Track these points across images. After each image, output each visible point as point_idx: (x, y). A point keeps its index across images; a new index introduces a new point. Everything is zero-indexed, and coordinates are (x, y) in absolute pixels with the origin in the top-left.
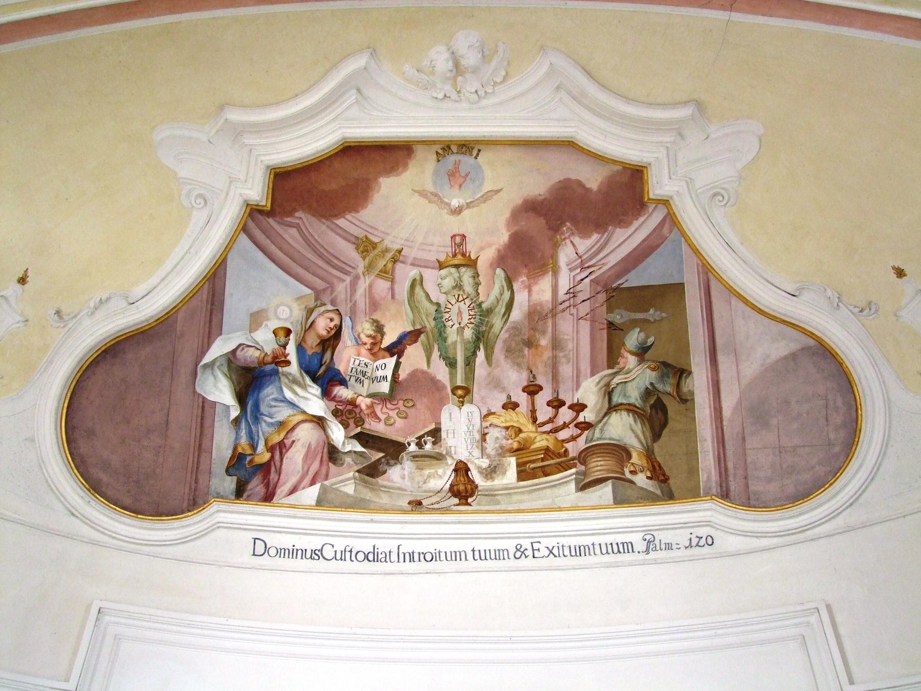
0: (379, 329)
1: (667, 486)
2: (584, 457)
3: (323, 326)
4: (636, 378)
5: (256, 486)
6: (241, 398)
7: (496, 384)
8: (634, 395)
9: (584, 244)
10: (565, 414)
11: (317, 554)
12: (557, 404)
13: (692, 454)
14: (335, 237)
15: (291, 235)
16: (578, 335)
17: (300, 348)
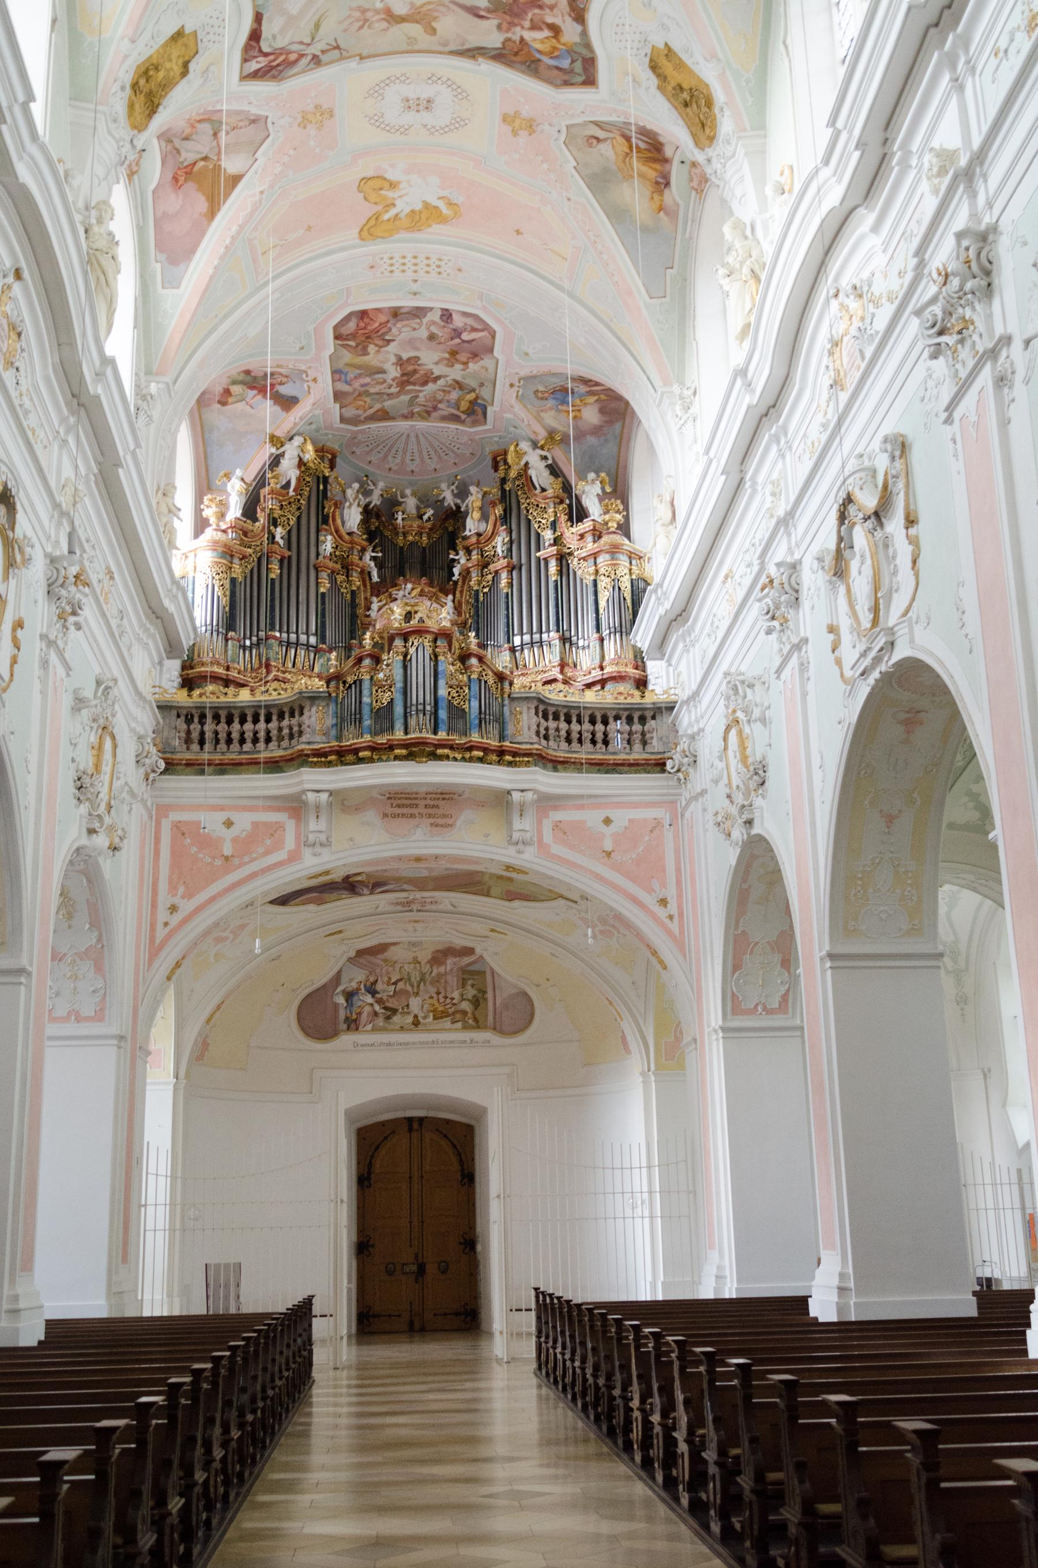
0: (390, 979)
1: (478, 1024)
2: (454, 1013)
3: (372, 979)
4: (471, 992)
5: (353, 1025)
6: (347, 1001)
8: (470, 997)
9: (455, 960)
10: (448, 1001)
11: (373, 1045)
13: (487, 1016)
14: (378, 960)
15: (361, 960)
16: (453, 981)
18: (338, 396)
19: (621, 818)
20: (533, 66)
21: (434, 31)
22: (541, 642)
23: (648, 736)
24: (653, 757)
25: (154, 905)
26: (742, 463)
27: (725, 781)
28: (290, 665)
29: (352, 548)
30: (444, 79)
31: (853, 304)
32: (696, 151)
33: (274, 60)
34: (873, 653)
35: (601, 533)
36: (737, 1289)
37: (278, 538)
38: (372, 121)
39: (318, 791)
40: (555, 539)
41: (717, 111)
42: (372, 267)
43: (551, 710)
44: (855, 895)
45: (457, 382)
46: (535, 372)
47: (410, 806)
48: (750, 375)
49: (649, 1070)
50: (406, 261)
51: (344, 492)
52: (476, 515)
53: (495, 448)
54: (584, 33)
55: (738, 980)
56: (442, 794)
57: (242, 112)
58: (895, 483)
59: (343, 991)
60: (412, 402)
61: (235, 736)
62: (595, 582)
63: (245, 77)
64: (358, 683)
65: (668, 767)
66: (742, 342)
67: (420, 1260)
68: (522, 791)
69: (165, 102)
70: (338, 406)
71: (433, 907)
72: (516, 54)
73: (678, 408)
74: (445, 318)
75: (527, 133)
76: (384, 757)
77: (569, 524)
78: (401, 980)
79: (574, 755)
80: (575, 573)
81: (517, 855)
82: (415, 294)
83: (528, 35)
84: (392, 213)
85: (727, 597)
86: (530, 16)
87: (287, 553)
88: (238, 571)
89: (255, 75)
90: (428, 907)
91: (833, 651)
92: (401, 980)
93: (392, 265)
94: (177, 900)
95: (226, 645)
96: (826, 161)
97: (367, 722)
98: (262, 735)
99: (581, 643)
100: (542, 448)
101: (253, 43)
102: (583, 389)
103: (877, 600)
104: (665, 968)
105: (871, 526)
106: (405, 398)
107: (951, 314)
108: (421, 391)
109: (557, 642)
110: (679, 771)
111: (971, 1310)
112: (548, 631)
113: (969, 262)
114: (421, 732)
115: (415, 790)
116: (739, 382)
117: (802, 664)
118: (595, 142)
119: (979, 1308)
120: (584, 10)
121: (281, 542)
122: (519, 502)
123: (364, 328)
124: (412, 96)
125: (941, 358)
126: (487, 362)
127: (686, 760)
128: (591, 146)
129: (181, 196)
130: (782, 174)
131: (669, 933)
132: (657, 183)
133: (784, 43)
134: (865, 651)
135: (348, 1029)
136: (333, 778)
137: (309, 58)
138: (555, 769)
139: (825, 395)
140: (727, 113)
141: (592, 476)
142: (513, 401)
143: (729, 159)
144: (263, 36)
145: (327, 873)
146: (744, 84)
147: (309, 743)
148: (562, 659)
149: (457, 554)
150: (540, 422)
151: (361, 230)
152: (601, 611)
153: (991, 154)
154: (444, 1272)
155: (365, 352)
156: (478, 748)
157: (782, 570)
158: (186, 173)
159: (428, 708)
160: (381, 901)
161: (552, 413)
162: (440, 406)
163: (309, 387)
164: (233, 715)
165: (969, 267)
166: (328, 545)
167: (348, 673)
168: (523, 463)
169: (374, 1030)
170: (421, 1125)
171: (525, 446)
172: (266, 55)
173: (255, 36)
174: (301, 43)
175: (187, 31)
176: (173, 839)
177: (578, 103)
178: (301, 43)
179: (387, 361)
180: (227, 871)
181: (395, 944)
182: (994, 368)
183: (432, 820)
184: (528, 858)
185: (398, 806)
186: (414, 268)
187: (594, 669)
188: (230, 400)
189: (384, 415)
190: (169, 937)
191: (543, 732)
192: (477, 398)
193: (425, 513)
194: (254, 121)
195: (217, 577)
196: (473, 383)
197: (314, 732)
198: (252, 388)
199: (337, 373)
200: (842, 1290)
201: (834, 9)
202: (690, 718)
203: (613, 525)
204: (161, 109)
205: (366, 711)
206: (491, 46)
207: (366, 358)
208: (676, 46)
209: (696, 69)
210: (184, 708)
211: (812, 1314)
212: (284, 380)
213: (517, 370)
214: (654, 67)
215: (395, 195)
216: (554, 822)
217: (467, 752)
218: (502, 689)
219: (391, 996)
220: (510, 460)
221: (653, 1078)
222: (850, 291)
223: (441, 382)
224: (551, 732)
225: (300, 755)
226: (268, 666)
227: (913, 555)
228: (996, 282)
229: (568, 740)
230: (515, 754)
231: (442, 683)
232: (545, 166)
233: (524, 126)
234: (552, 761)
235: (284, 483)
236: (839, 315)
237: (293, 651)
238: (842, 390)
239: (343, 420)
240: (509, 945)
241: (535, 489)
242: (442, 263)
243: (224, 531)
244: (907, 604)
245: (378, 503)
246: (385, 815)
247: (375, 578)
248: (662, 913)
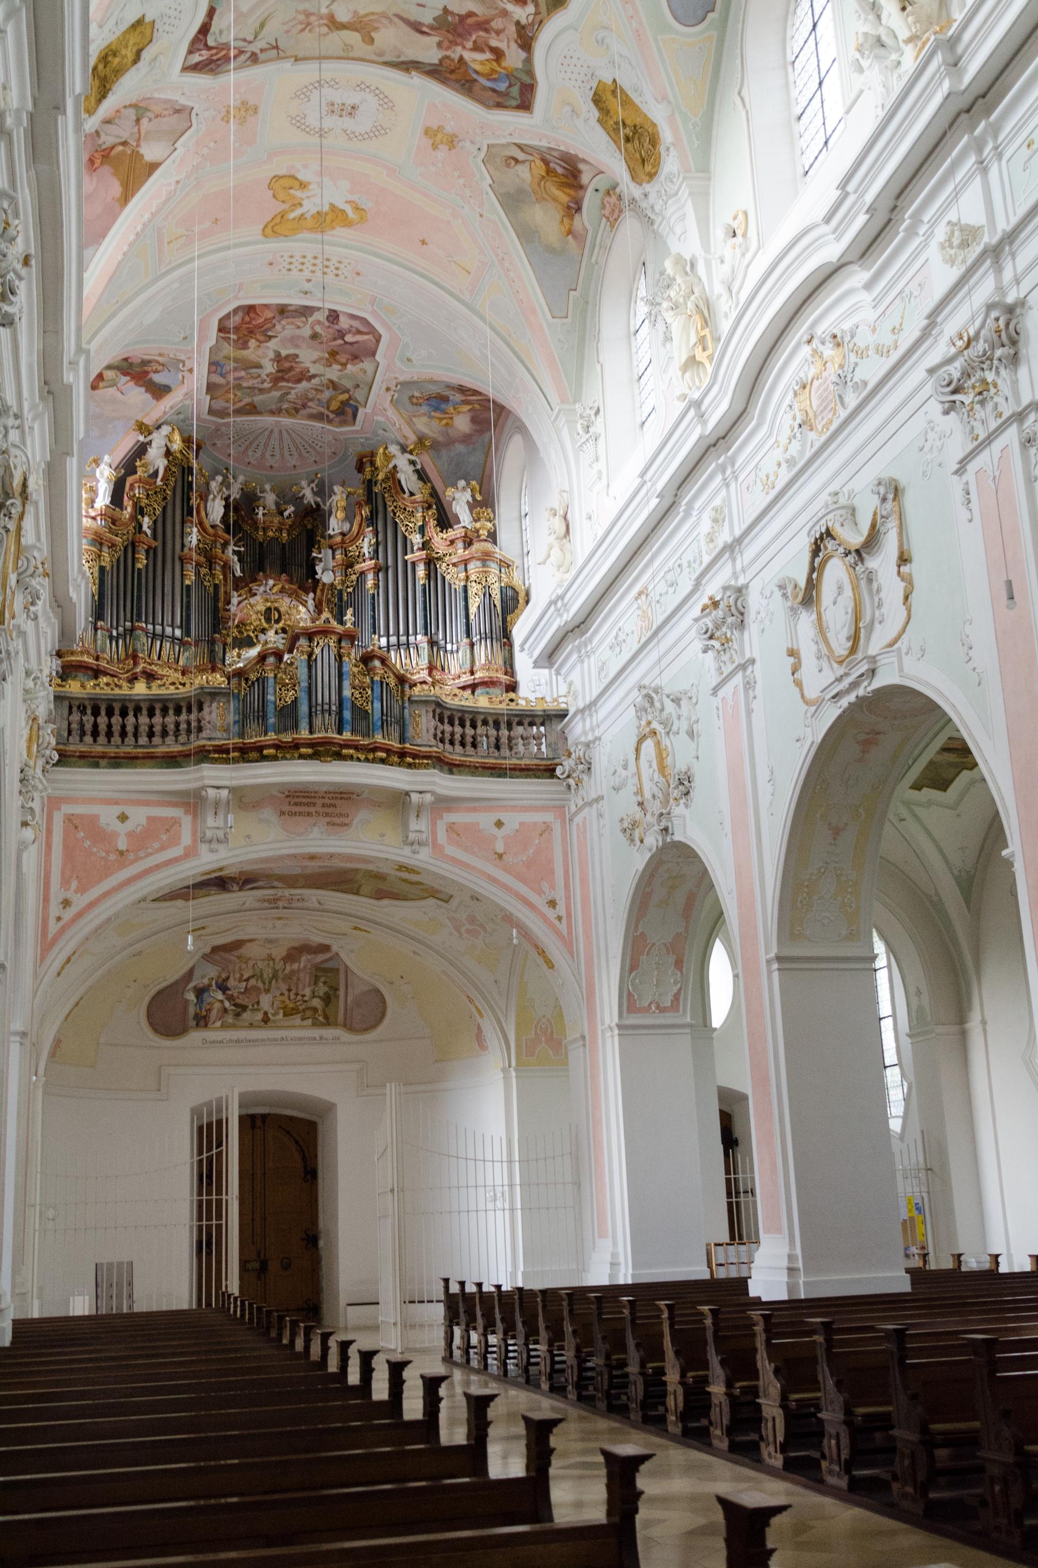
0: (242, 975)
1: (328, 1022)
2: (304, 1011)
3: (224, 976)
4: (322, 989)
5: (202, 1023)
6: (197, 997)
7: (278, 988)
8: (321, 994)
10: (299, 998)
11: (221, 1042)
12: (297, 994)
15: (217, 957)
17: (216, 983)
18: (211, 388)
19: (513, 820)
20: (467, 85)
21: (372, 41)
22: (408, 644)
23: (513, 742)
24: (544, 763)
25: (46, 899)
26: (679, 489)
27: (631, 787)
28: (156, 658)
29: (215, 541)
30: (373, 88)
31: (828, 351)
32: (632, 185)
33: (216, 54)
34: (851, 679)
35: (471, 540)
36: (633, 1275)
37: (145, 528)
38: (294, 122)
39: (218, 788)
40: (423, 544)
41: (662, 149)
42: (271, 264)
43: (447, 713)
44: (801, 902)
45: (331, 381)
46: (415, 378)
47: (308, 804)
48: (703, 408)
49: (510, 1066)
50: (305, 260)
51: (208, 484)
52: (341, 515)
53: (360, 449)
54: (529, 61)
55: (634, 979)
56: (341, 793)
57: (170, 101)
58: (883, 524)
59: (195, 987)
60: (282, 399)
61: (130, 729)
62: (465, 587)
63: (188, 68)
64: (262, 681)
65: (559, 771)
66: (684, 373)
67: (262, 1257)
68: (421, 792)
69: (114, 88)
70: (209, 397)
71: (300, 904)
72: (452, 72)
73: (579, 426)
74: (331, 319)
75: (447, 148)
76: (288, 756)
77: (439, 529)
78: (253, 976)
79: (469, 759)
80: (444, 578)
81: (412, 855)
82: (306, 293)
83: (468, 56)
84: (297, 212)
85: (640, 612)
86: (474, 37)
87: (154, 544)
88: (107, 560)
89: (196, 68)
90: (294, 905)
91: (793, 674)
92: (253, 976)
93: (291, 263)
94: (69, 895)
95: (96, 634)
96: (827, 220)
97: (272, 721)
98: (157, 729)
99: (449, 647)
100: (411, 452)
101: (201, 37)
102: (458, 397)
103: (857, 630)
104: (550, 965)
105: (852, 561)
106: (276, 394)
107: (969, 376)
108: (293, 388)
109: (425, 645)
110: (568, 776)
111: (904, 1285)
112: (416, 634)
113: (1000, 331)
114: (327, 732)
115: (317, 789)
116: (692, 412)
117: (748, 683)
118: (513, 163)
119: (912, 1284)
120: (532, 38)
121: (149, 532)
122: (385, 504)
123: (248, 323)
124: (338, 101)
125: (952, 413)
126: (367, 365)
127: (581, 767)
128: (508, 166)
129: (95, 179)
130: (735, 218)
131: (558, 933)
132: (569, 207)
133: (739, 94)
134: (841, 676)
135: (197, 1025)
136: (227, 774)
137: (248, 55)
138: (451, 772)
139: (786, 432)
140: (673, 152)
141: (462, 483)
142: (387, 404)
143: (671, 197)
144: (211, 31)
145: (221, 869)
146: (691, 127)
147: (210, 739)
148: (430, 662)
149: (320, 553)
150: (410, 426)
151: (266, 226)
152: (472, 617)
153: (1023, 236)
154: (286, 1269)
155: (245, 346)
156: (382, 750)
157: (728, 593)
158: (103, 156)
159: (334, 708)
160: (249, 897)
161: (424, 419)
162: (310, 404)
163: (183, 377)
164: (127, 708)
165: (1000, 336)
166: (194, 537)
167: (252, 669)
168: (391, 466)
169: (225, 1026)
170: (264, 1122)
171: (394, 449)
172: (209, 48)
173: (205, 29)
174: (245, 40)
175: (147, 20)
176: (66, 832)
177: (509, 126)
178: (245, 40)
179: (265, 356)
180: (122, 866)
181: (250, 941)
182: (1021, 431)
183: (328, 819)
184: (423, 858)
185: (296, 804)
186: (311, 268)
187: (465, 673)
188: (101, 385)
189: (252, 409)
190: (62, 931)
191: (439, 735)
192: (350, 398)
193: (286, 510)
194: (178, 111)
195: (87, 565)
196: (348, 384)
197: (214, 727)
198: (125, 374)
199: (214, 365)
200: (792, 1271)
201: (790, 68)
202: (584, 726)
203: (484, 533)
204: (110, 95)
205: (270, 709)
206: (427, 61)
207: (245, 352)
208: (624, 82)
209: (644, 108)
210: (77, 699)
211: (752, 1293)
212: (160, 368)
213: (397, 375)
214: (597, 100)
215: (303, 195)
216: (452, 826)
217: (371, 753)
218: (403, 692)
219: (242, 993)
220: (378, 463)
221: (514, 1074)
222: (828, 339)
223: (314, 381)
224: (447, 736)
225: (201, 751)
226: (135, 657)
227: (905, 591)
228: (1023, 352)
229: (463, 744)
230: (415, 756)
231: (346, 684)
232: (461, 181)
233: (445, 141)
234: (448, 764)
235: (151, 472)
236: (810, 360)
237: (158, 643)
238: (811, 430)
239: (211, 411)
240: (365, 941)
241: (404, 492)
242: (342, 266)
243: (94, 518)
244: (894, 634)
245: (238, 497)
246: (282, 813)
247: (238, 573)
248: (551, 914)
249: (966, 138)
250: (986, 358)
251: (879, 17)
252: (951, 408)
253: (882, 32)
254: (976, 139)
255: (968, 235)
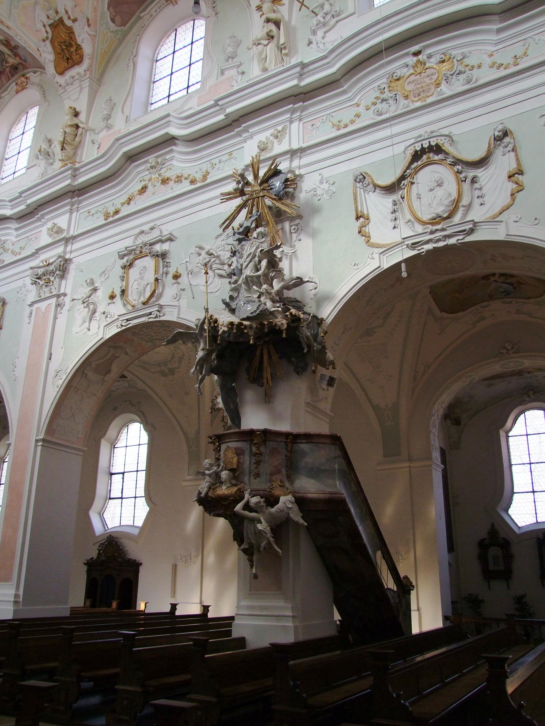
96: (10, 201)
182: (57, 301)
249: (69, 200)
250: (53, 273)
251: (50, 145)
252: (35, 283)
253: (50, 150)
254: (72, 202)
255: (60, 231)
